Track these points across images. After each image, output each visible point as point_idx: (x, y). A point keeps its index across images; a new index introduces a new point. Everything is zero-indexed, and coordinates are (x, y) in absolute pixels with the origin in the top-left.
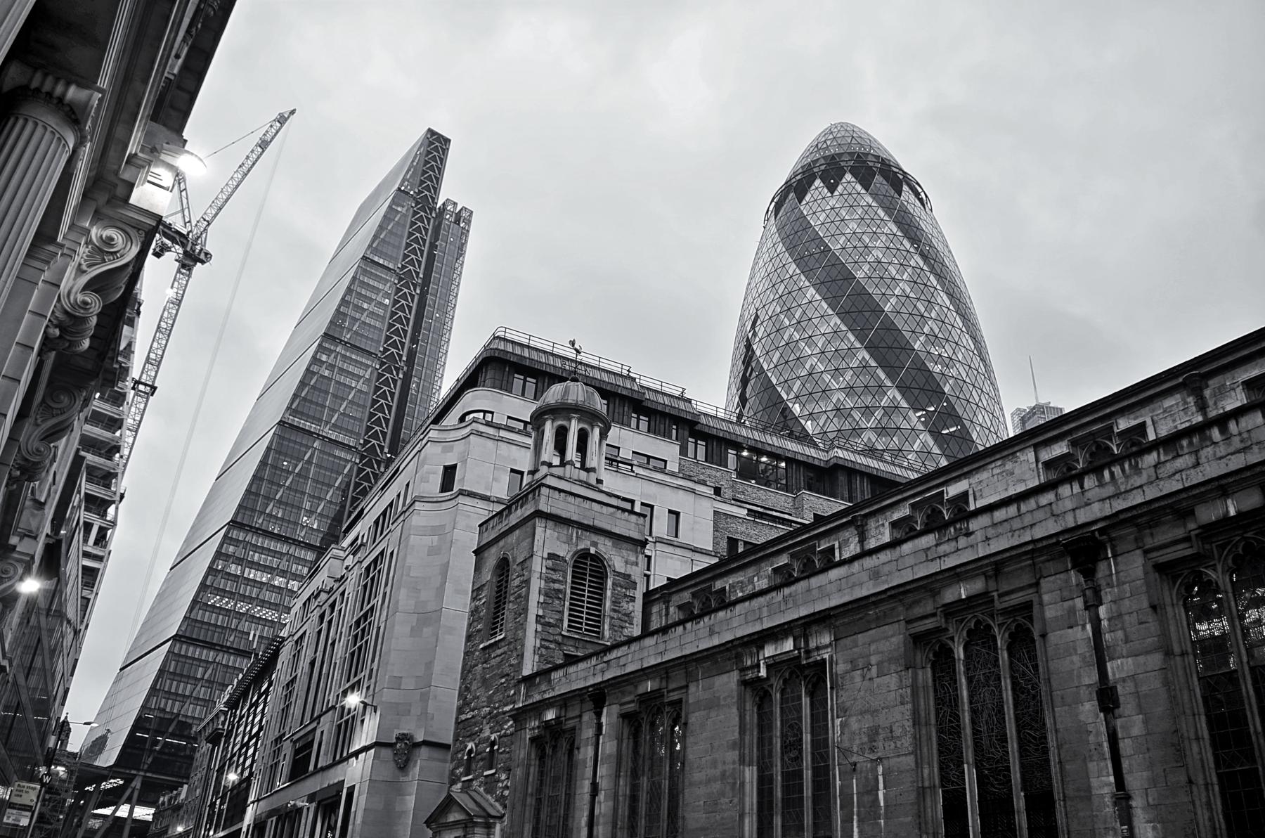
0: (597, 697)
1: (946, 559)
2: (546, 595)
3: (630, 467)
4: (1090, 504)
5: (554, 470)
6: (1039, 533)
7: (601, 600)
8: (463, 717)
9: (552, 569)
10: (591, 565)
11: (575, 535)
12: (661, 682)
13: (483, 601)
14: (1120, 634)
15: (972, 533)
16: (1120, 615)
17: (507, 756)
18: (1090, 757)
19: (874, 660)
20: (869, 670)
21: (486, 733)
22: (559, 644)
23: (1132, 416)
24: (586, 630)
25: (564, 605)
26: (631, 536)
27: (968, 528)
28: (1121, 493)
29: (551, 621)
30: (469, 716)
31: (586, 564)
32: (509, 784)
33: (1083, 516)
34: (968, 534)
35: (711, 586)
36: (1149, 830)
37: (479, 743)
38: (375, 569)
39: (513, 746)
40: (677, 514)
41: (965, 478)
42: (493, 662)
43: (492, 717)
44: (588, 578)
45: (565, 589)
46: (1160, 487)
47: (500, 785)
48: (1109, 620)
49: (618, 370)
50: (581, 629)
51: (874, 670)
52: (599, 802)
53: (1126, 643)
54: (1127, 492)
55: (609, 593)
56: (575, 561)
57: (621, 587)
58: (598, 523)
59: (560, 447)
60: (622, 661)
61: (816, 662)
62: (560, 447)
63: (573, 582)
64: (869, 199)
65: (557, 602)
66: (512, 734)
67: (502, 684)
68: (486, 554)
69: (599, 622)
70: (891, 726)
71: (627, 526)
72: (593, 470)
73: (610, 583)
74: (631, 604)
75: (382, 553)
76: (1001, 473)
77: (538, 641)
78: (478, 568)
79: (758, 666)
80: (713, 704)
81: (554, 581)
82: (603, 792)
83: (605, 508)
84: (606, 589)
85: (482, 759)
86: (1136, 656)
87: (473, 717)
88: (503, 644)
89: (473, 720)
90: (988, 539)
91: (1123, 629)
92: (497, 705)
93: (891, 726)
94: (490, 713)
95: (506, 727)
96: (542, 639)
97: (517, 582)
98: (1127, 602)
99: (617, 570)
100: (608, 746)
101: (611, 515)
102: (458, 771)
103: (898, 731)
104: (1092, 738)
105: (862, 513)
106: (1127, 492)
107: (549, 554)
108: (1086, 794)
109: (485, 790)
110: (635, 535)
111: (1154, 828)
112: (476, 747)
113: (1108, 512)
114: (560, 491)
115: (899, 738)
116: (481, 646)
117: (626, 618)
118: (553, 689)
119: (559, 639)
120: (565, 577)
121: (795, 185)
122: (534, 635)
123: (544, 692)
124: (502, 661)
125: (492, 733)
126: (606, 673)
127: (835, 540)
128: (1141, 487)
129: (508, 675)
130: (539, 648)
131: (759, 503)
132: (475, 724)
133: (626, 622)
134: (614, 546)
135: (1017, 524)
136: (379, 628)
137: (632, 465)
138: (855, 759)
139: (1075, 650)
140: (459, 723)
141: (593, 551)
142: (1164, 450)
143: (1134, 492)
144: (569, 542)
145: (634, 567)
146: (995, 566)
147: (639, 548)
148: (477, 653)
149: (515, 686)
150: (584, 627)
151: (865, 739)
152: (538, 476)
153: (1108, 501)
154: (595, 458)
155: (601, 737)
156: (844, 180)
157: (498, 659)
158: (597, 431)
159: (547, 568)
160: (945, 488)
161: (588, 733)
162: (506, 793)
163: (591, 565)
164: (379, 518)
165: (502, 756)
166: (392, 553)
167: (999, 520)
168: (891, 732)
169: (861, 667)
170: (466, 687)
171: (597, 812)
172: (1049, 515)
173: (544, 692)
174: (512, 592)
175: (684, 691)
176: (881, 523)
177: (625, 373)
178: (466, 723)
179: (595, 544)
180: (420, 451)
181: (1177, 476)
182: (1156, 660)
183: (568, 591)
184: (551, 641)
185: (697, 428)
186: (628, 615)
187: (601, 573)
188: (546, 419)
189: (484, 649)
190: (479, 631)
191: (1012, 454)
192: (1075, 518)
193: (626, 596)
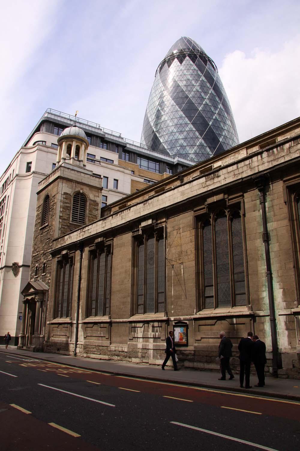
0: (80, 245)
1: (209, 187)
2: (63, 208)
3: (99, 163)
4: (264, 164)
5: (67, 161)
6: (244, 175)
7: (85, 210)
8: (34, 255)
9: (65, 199)
10: (81, 197)
11: (74, 185)
12: (104, 238)
13: (40, 211)
14: (272, 213)
15: (220, 176)
16: (273, 206)
17: (50, 268)
18: (258, 259)
19: (181, 226)
20: (179, 230)
21: (42, 260)
23: (283, 136)
24: (79, 221)
25: (70, 212)
26: (96, 186)
27: (218, 174)
28: (276, 159)
29: (65, 218)
30: (36, 254)
31: (79, 197)
32: (50, 278)
33: (261, 168)
34: (218, 177)
36: (278, 285)
38: (3, 203)
39: (51, 264)
40: (117, 180)
41: (220, 161)
42: (44, 234)
43: (44, 254)
44: (80, 202)
45: (71, 206)
46: (291, 156)
47: (48, 278)
48: (269, 208)
49: (95, 126)
50: (77, 221)
51: (181, 230)
52: (82, 283)
53: (274, 216)
54: (278, 158)
55: (88, 207)
56: (75, 196)
57: (93, 205)
58: (84, 181)
59: (69, 152)
60: (89, 231)
61: (160, 228)
62: (69, 152)
63: (74, 203)
65: (68, 211)
66: (51, 260)
67: (47, 242)
68: (41, 194)
69: (84, 218)
70: (187, 251)
71: (94, 182)
72: (82, 161)
73: (88, 204)
74: (96, 212)
75: (5, 197)
76: (234, 158)
77: (60, 225)
78: (38, 199)
79: (139, 230)
80: (122, 245)
81: (66, 203)
82: (83, 279)
83: (86, 175)
84: (87, 206)
85: (41, 270)
86: (277, 221)
87: (37, 254)
88: (48, 227)
89: (38, 256)
90: (225, 178)
91: (273, 211)
92: (46, 250)
93: (187, 251)
94: (43, 253)
95: (49, 257)
96: (62, 225)
97: (52, 204)
98: (275, 201)
99: (91, 199)
100: (85, 263)
101: (88, 178)
102: (33, 274)
103: (189, 252)
104: (259, 252)
105: (182, 175)
106: (278, 158)
107: (64, 193)
108: (256, 273)
109: (42, 280)
110: (98, 186)
111: (280, 284)
112: (39, 265)
113: (271, 166)
114: (68, 169)
115: (189, 255)
116: (40, 228)
117: (95, 217)
118: (65, 243)
119: (69, 224)
120: (70, 201)
121: (167, 60)
122: (59, 223)
123: (62, 244)
124: (47, 233)
125: (44, 260)
126: (84, 236)
127: (172, 185)
128: (284, 156)
129: (49, 238)
130: (61, 228)
131: (148, 177)
132: (38, 257)
133: (94, 218)
134: (90, 189)
135: (236, 172)
136: (5, 224)
137: (100, 162)
138: (173, 263)
139: (255, 220)
141: (81, 191)
142: (293, 142)
143: (281, 158)
144: (72, 188)
145: (98, 198)
146: (228, 189)
147: (100, 190)
148: (38, 231)
149: (52, 242)
150: (78, 220)
151: (177, 256)
152: (60, 163)
153: (271, 162)
154: (83, 157)
155: (82, 259)
156: (185, 59)
157: (46, 233)
158: (83, 147)
159: (63, 198)
160: (213, 165)
161: (78, 258)
162: (50, 281)
163: (81, 197)
164: (4, 184)
166: (9, 196)
167: (230, 171)
168: (187, 253)
169: (176, 229)
170: (35, 244)
171: (81, 287)
172: (248, 168)
173: (62, 244)
174: (51, 207)
175: (112, 241)
176: (189, 178)
177: (98, 127)
179: (82, 189)
180: (18, 157)
181: (298, 152)
182: (286, 222)
183: (72, 207)
184: (65, 226)
185: (125, 149)
186: (95, 216)
187: (85, 200)
188: (63, 142)
189: (41, 229)
190: (39, 223)
191: (238, 151)
192: (258, 169)
193: (94, 209)
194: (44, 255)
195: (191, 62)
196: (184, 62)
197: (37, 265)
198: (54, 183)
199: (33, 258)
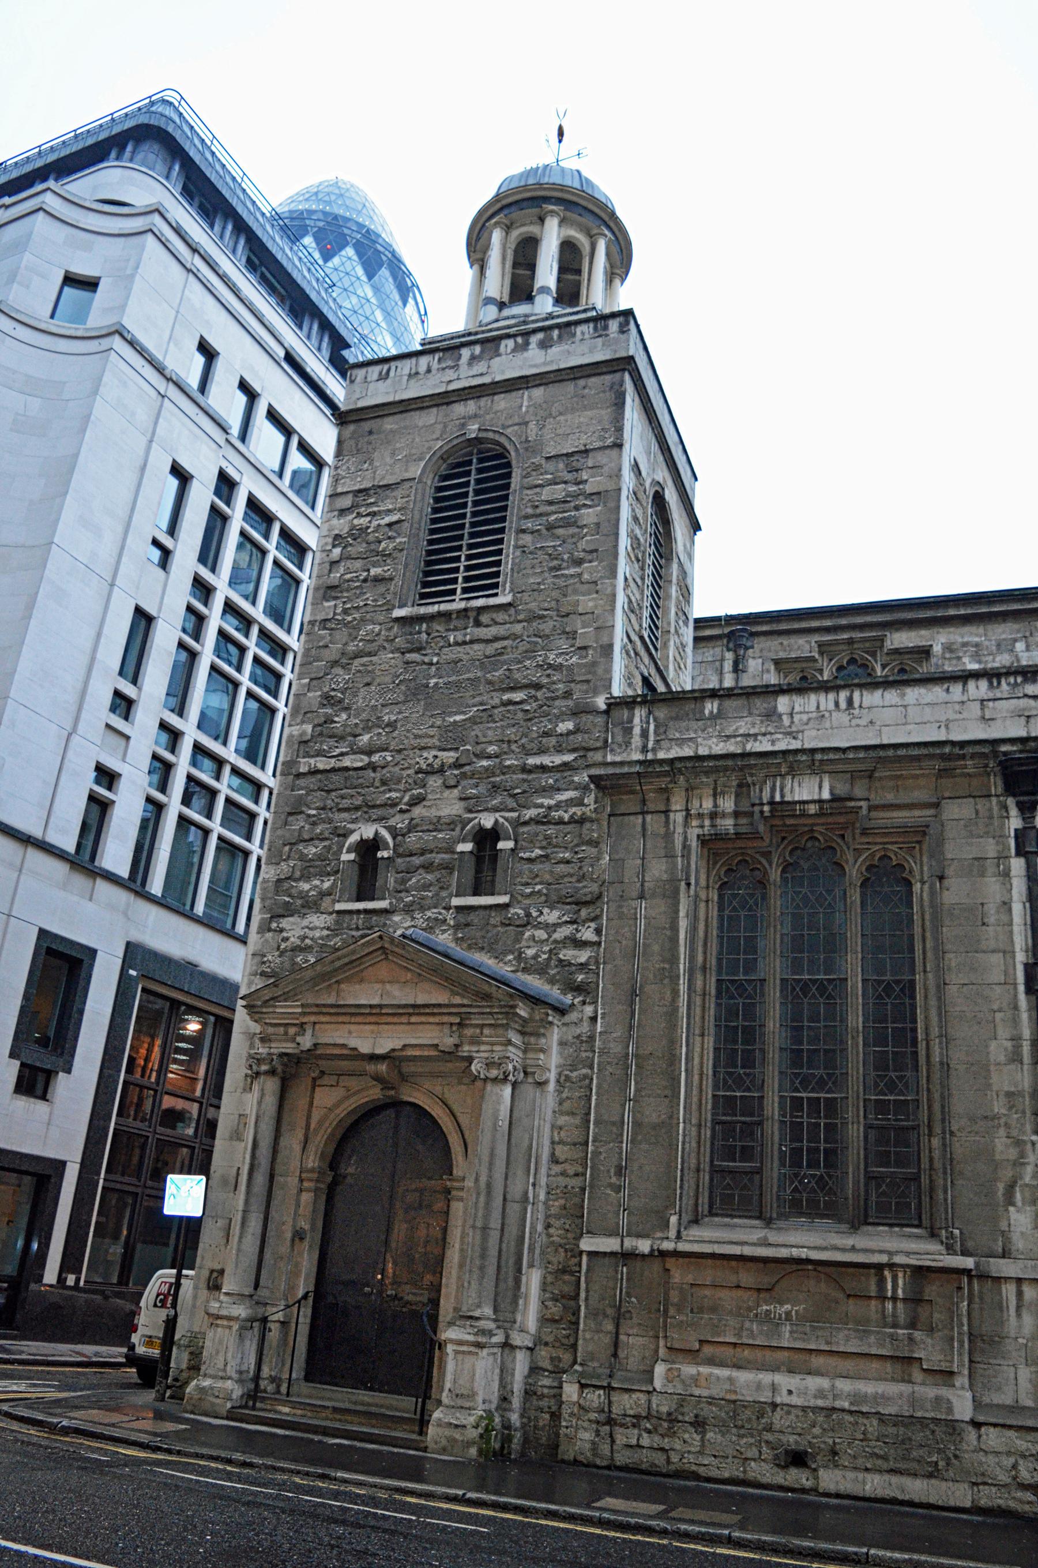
22: (636, 654)
35: (882, 640)
37: (411, 828)
64: (369, 293)
66: (581, 821)
88: (501, 617)
92: (492, 749)
94: (457, 765)
102: (306, 886)
129: (538, 686)
140: (299, 775)
156: (343, 253)
157: (490, 649)
165: (536, 867)
178: (335, 777)
194: (464, 775)
195: (360, 271)
196: (336, 261)
197: (368, 831)
198: (570, 387)
199: (301, 782)
